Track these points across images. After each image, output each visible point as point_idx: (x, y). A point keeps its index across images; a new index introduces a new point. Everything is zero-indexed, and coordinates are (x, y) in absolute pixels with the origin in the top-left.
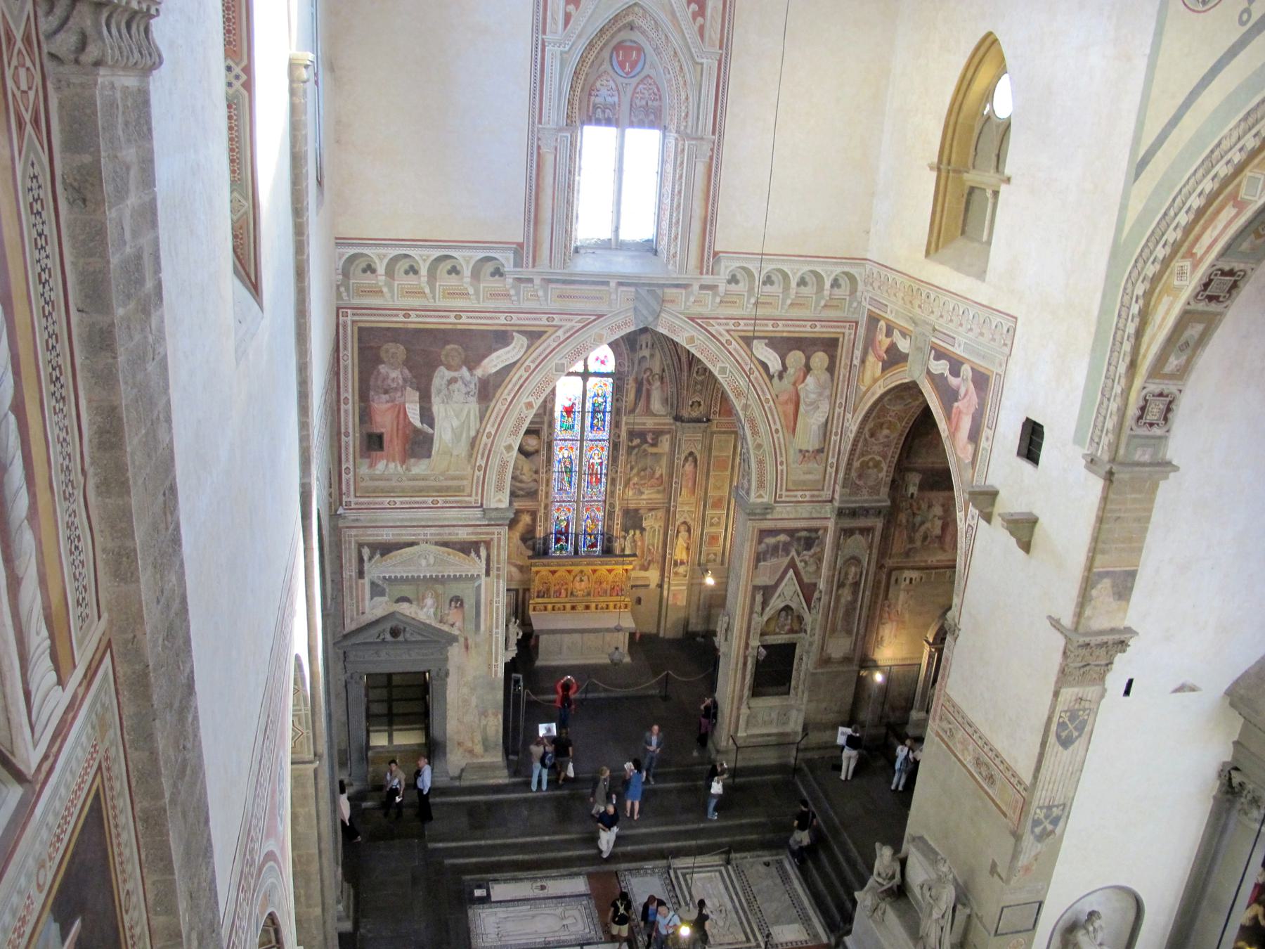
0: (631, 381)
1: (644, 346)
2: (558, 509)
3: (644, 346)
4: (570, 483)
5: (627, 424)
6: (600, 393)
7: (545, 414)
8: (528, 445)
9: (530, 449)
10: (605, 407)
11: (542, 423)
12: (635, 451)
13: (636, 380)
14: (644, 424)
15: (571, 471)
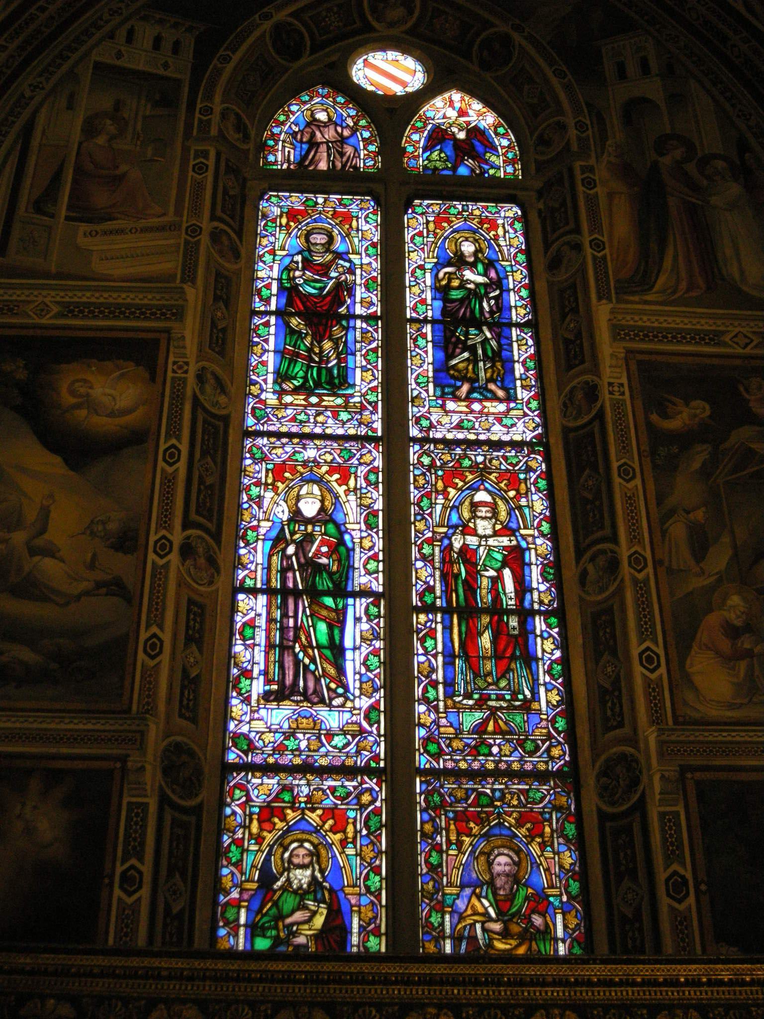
0: (602, 173)
1: (632, 68)
2: (269, 813)
3: (632, 68)
4: (337, 650)
5: (618, 332)
6: (468, 248)
7: (189, 276)
8: (88, 403)
9: (102, 424)
10: (501, 306)
11: (179, 314)
12: (699, 456)
13: (625, 171)
14: (714, 338)
15: (341, 591)
